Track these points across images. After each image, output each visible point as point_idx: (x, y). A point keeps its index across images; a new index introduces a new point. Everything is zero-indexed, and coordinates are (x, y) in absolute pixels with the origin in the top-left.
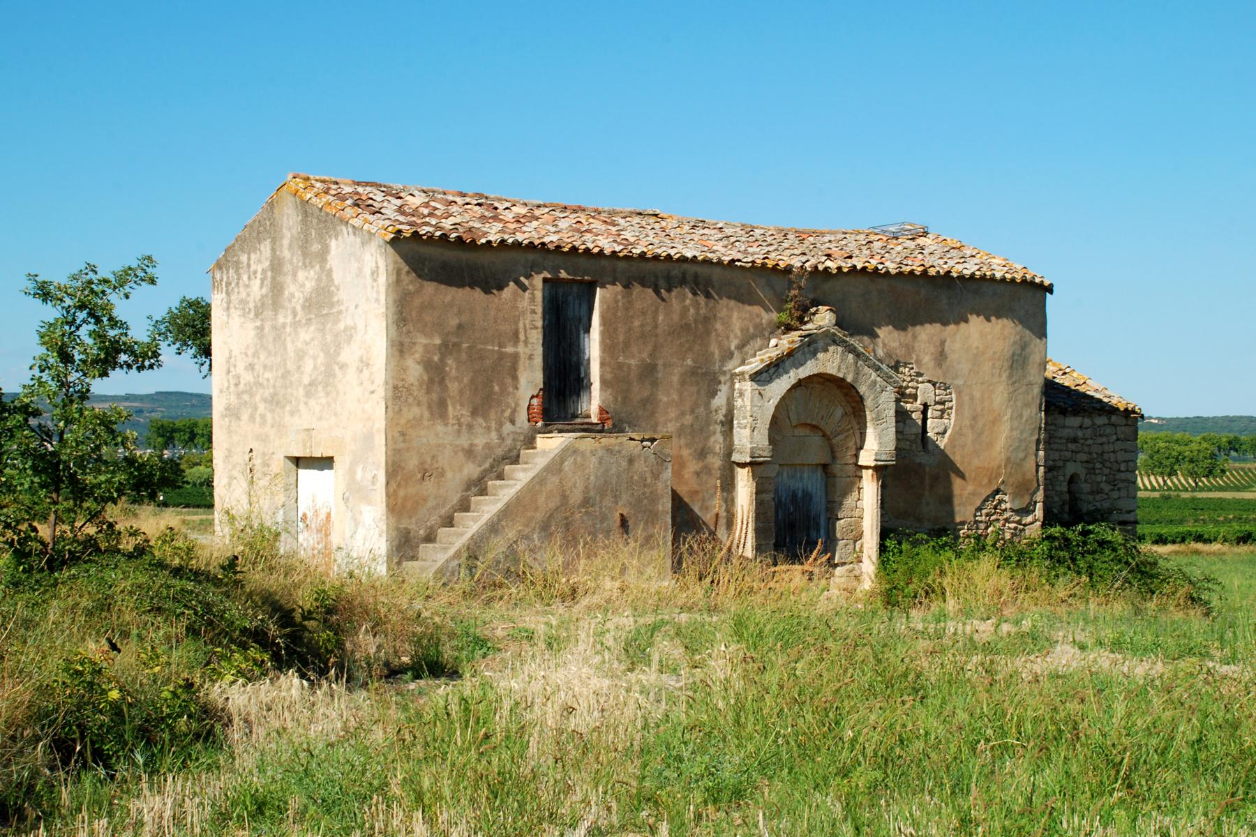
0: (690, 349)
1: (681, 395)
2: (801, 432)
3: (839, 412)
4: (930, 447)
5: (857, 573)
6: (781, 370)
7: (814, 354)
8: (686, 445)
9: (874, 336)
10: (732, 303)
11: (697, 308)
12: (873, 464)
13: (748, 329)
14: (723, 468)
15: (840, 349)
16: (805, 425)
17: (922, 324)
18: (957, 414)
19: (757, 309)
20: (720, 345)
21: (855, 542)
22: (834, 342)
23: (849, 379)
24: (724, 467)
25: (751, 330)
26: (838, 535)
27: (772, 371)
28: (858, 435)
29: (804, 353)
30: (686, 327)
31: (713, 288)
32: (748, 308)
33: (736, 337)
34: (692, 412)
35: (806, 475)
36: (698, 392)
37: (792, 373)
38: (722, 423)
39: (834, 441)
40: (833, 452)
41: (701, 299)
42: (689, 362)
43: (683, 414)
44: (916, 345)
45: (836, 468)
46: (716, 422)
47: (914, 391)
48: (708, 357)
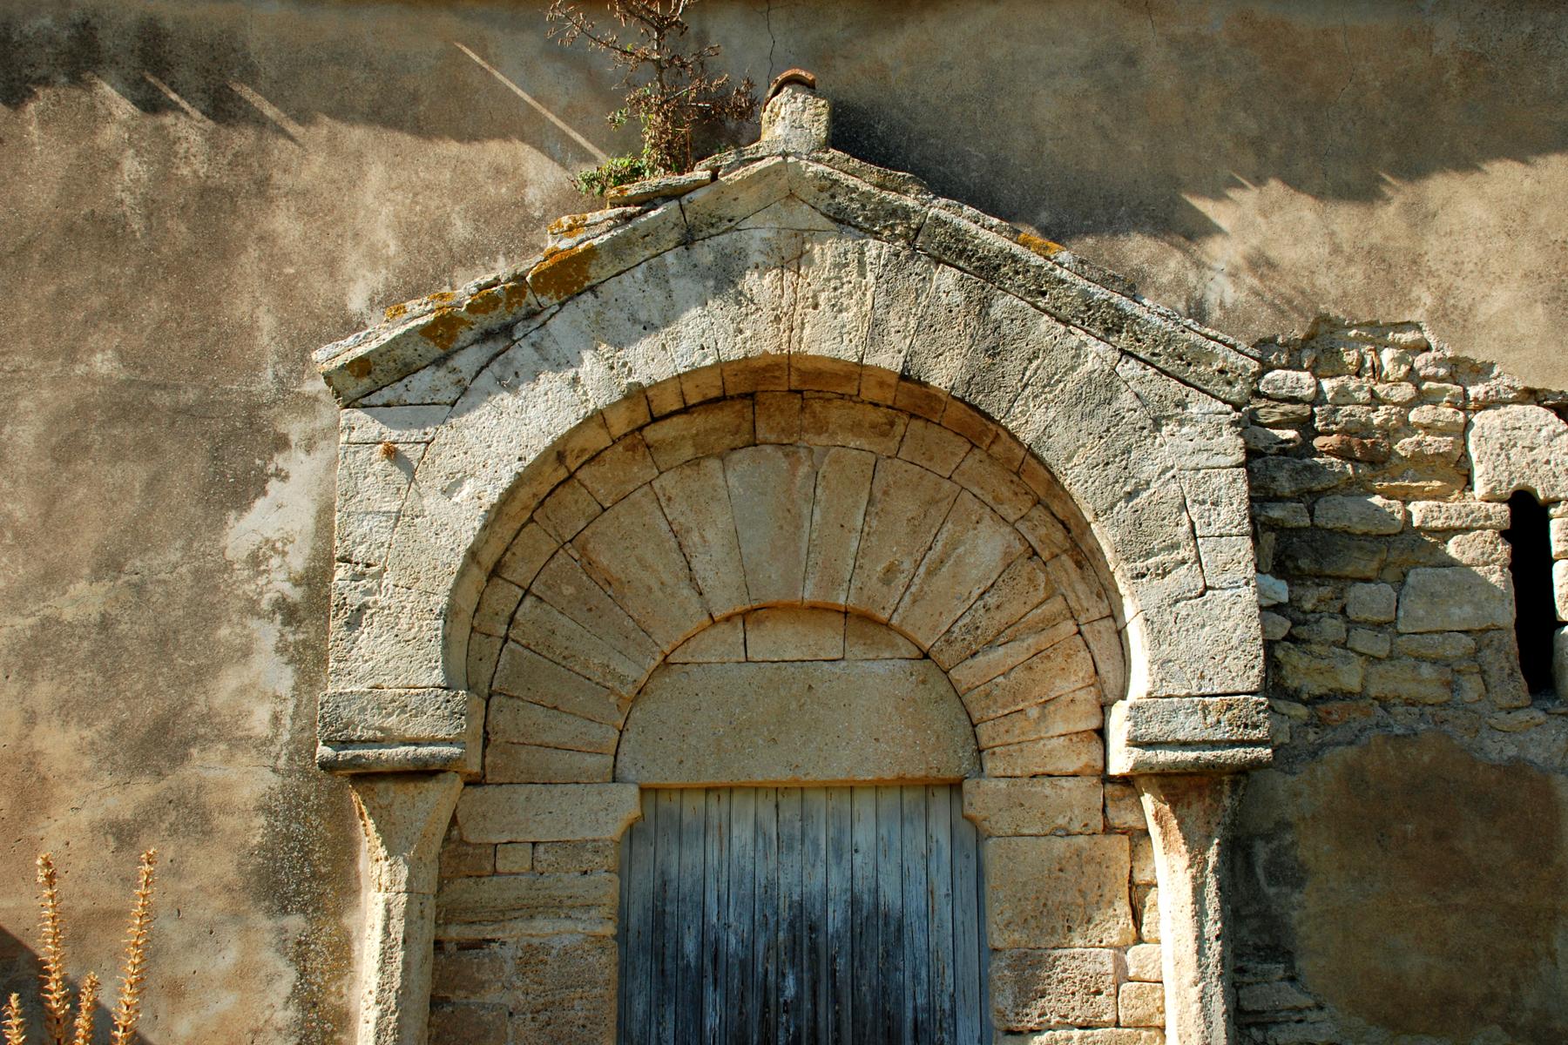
0: (116, 312)
1: (50, 502)
2: (781, 642)
3: (987, 547)
6: (523, 353)
7: (724, 278)
8: (66, 710)
9: (1196, 231)
10: (356, 135)
11: (166, 153)
13: (439, 229)
14: (285, 809)
15: (872, 247)
16: (818, 610)
17: (1464, 162)
19: (495, 151)
20: (286, 292)
22: (841, 220)
23: (943, 374)
24: (294, 805)
25: (460, 230)
27: (467, 360)
29: (659, 277)
30: (107, 232)
31: (250, 74)
32: (452, 148)
33: (374, 257)
34: (109, 565)
35: (864, 835)
36: (153, 484)
37: (591, 367)
38: (289, 613)
39: (964, 675)
41: (189, 129)
42: (104, 364)
43: (53, 577)
44: (1433, 247)
46: (252, 608)
47: (1437, 444)
48: (221, 346)
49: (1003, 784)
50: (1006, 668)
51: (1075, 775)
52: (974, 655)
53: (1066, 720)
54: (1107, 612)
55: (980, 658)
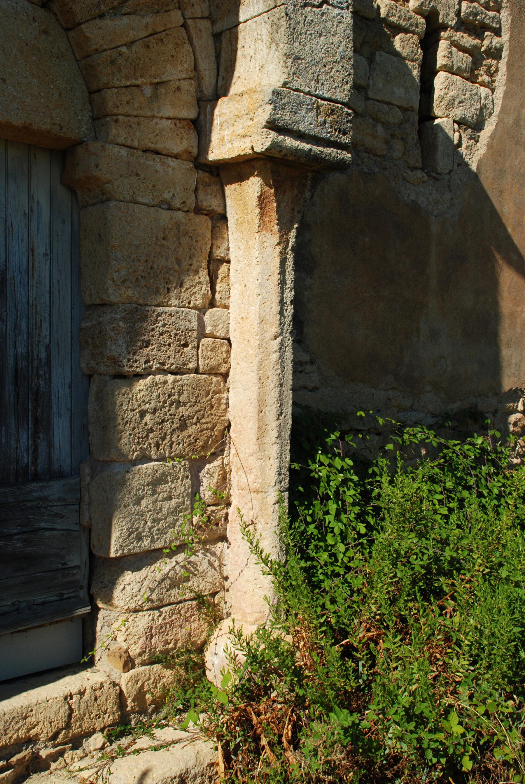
4: (443, 164)
5: (203, 585)
12: (262, 141)
18: (510, 79)
21: (196, 467)
26: (127, 443)
28: (204, 43)
39: (97, 33)
40: (94, 92)
45: (109, 161)
49: (124, 152)
50: (128, 40)
51: (176, 157)
52: (101, 16)
53: (173, 105)
54: (206, 14)
55: (107, 22)
